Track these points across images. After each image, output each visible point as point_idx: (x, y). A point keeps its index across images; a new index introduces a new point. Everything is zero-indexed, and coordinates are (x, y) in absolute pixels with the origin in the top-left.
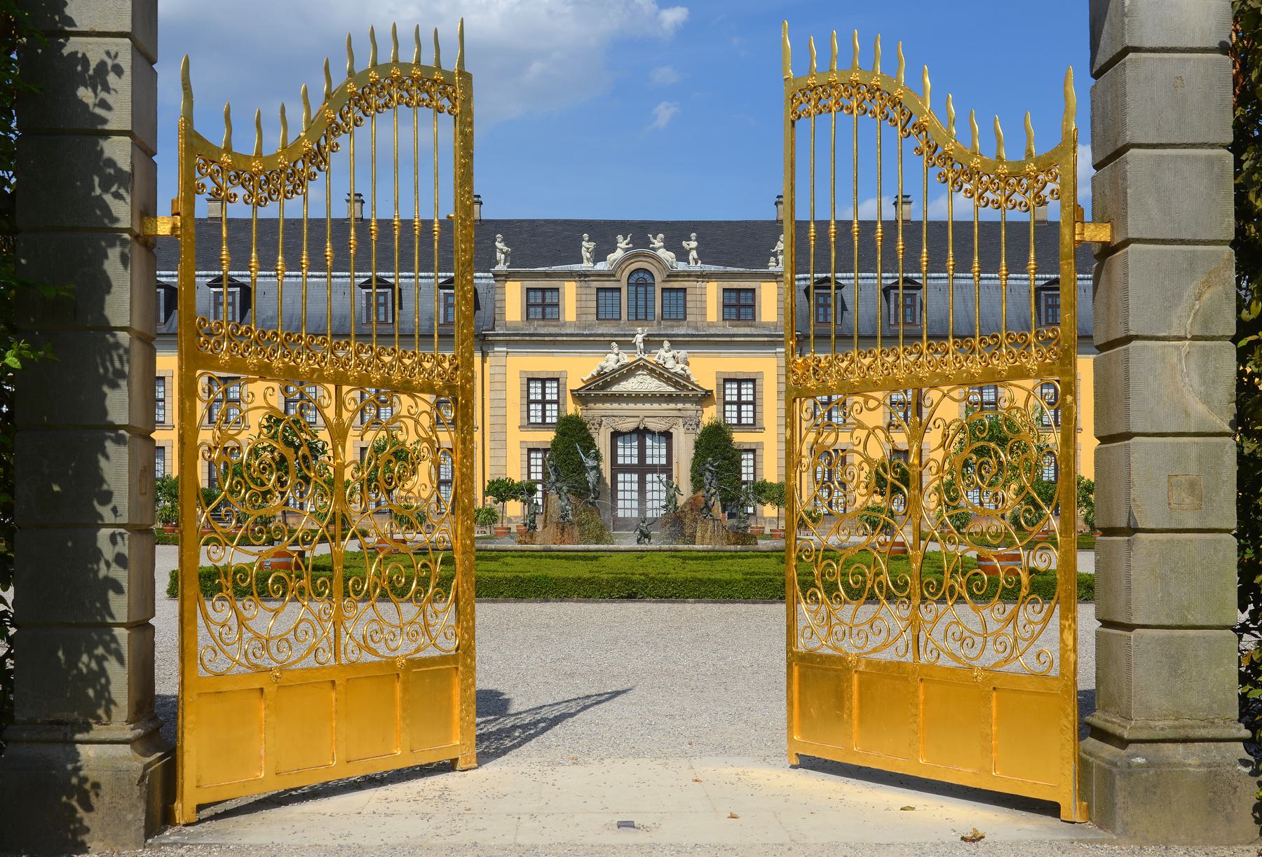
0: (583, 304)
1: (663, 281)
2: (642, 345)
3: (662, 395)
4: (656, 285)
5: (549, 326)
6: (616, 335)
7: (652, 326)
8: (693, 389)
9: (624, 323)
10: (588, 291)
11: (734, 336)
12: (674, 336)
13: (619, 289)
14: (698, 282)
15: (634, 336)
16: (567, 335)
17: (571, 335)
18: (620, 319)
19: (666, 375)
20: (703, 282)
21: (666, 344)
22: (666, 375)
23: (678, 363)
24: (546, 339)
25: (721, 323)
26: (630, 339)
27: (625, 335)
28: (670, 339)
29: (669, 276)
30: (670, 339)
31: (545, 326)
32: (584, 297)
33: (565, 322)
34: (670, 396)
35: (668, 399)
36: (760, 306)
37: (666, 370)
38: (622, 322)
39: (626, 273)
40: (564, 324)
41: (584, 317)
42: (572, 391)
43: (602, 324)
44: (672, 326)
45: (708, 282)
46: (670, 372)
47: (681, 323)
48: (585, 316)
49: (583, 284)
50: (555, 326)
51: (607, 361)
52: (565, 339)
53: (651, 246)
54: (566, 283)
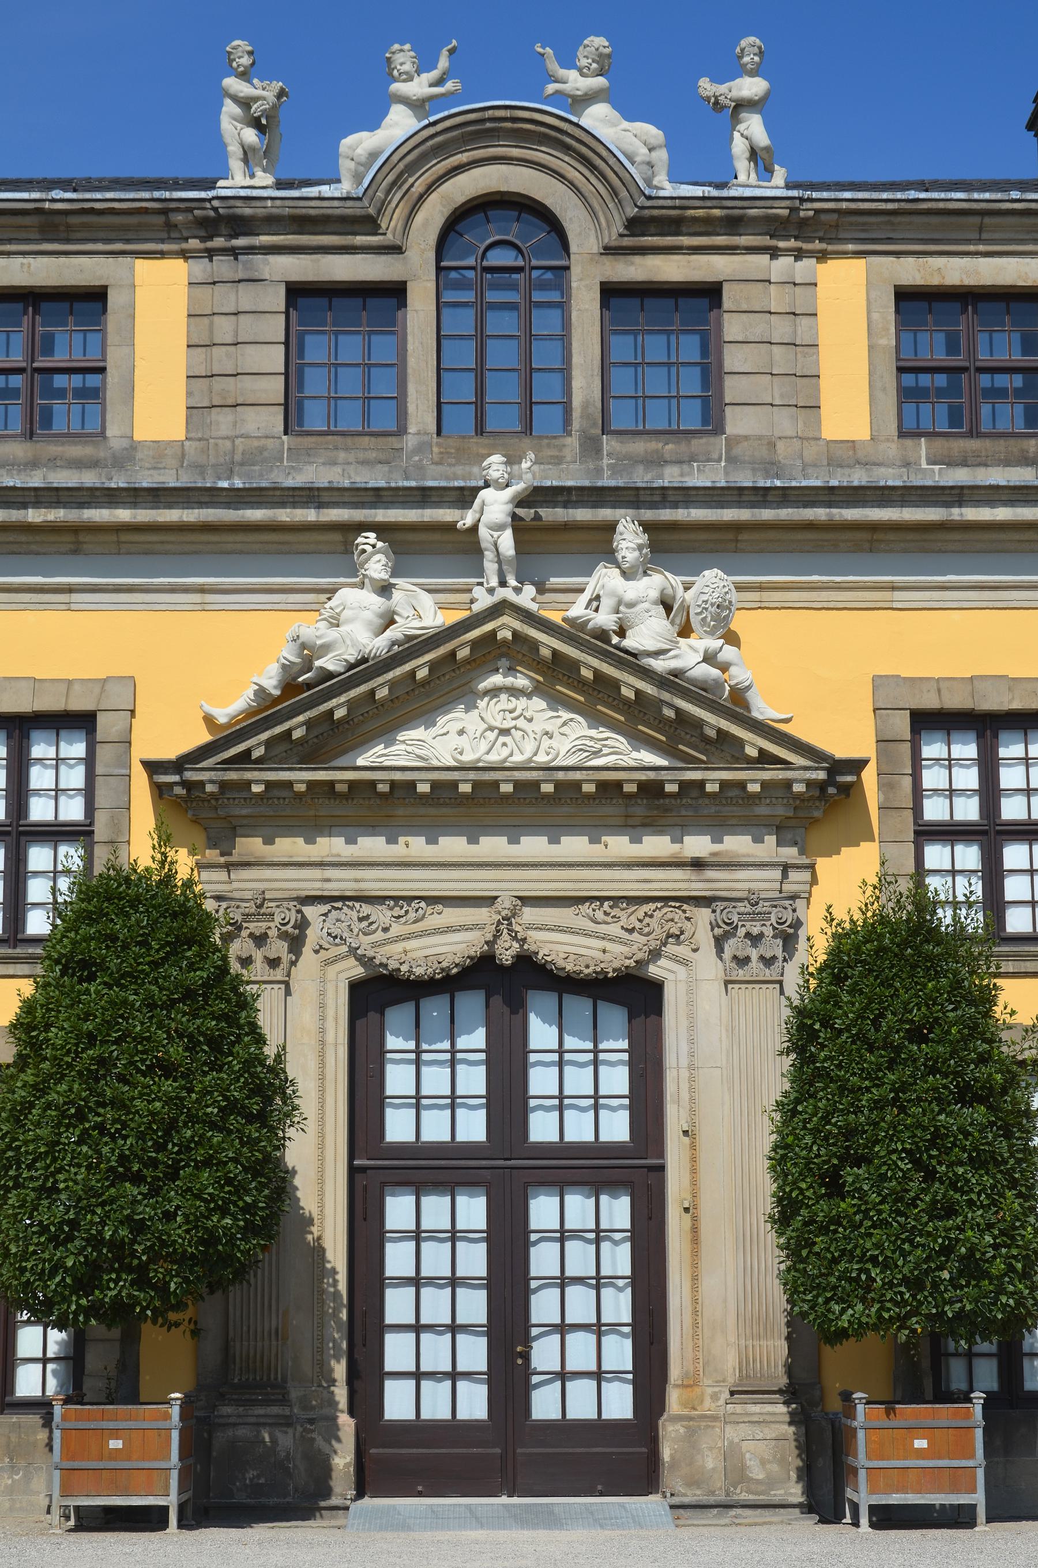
0: (222, 360)
1: (610, 251)
3: (609, 789)
4: (576, 271)
5: (53, 463)
6: (378, 497)
7: (558, 461)
9: (420, 449)
10: (246, 298)
11: (960, 495)
12: (665, 496)
14: (774, 253)
15: (465, 497)
16: (135, 496)
17: (157, 496)
18: (401, 431)
20: (799, 255)
23: (685, 631)
24: (34, 516)
25: (892, 448)
26: (445, 515)
27: (424, 496)
28: (648, 515)
30: (648, 515)
31: (33, 464)
32: (224, 329)
33: (134, 446)
34: (651, 790)
38: (410, 441)
40: (122, 460)
41: (223, 422)
42: (152, 767)
43: (309, 452)
44: (657, 462)
46: (646, 673)
47: (698, 444)
49: (223, 266)
50: (78, 464)
52: (124, 515)
53: (551, 88)
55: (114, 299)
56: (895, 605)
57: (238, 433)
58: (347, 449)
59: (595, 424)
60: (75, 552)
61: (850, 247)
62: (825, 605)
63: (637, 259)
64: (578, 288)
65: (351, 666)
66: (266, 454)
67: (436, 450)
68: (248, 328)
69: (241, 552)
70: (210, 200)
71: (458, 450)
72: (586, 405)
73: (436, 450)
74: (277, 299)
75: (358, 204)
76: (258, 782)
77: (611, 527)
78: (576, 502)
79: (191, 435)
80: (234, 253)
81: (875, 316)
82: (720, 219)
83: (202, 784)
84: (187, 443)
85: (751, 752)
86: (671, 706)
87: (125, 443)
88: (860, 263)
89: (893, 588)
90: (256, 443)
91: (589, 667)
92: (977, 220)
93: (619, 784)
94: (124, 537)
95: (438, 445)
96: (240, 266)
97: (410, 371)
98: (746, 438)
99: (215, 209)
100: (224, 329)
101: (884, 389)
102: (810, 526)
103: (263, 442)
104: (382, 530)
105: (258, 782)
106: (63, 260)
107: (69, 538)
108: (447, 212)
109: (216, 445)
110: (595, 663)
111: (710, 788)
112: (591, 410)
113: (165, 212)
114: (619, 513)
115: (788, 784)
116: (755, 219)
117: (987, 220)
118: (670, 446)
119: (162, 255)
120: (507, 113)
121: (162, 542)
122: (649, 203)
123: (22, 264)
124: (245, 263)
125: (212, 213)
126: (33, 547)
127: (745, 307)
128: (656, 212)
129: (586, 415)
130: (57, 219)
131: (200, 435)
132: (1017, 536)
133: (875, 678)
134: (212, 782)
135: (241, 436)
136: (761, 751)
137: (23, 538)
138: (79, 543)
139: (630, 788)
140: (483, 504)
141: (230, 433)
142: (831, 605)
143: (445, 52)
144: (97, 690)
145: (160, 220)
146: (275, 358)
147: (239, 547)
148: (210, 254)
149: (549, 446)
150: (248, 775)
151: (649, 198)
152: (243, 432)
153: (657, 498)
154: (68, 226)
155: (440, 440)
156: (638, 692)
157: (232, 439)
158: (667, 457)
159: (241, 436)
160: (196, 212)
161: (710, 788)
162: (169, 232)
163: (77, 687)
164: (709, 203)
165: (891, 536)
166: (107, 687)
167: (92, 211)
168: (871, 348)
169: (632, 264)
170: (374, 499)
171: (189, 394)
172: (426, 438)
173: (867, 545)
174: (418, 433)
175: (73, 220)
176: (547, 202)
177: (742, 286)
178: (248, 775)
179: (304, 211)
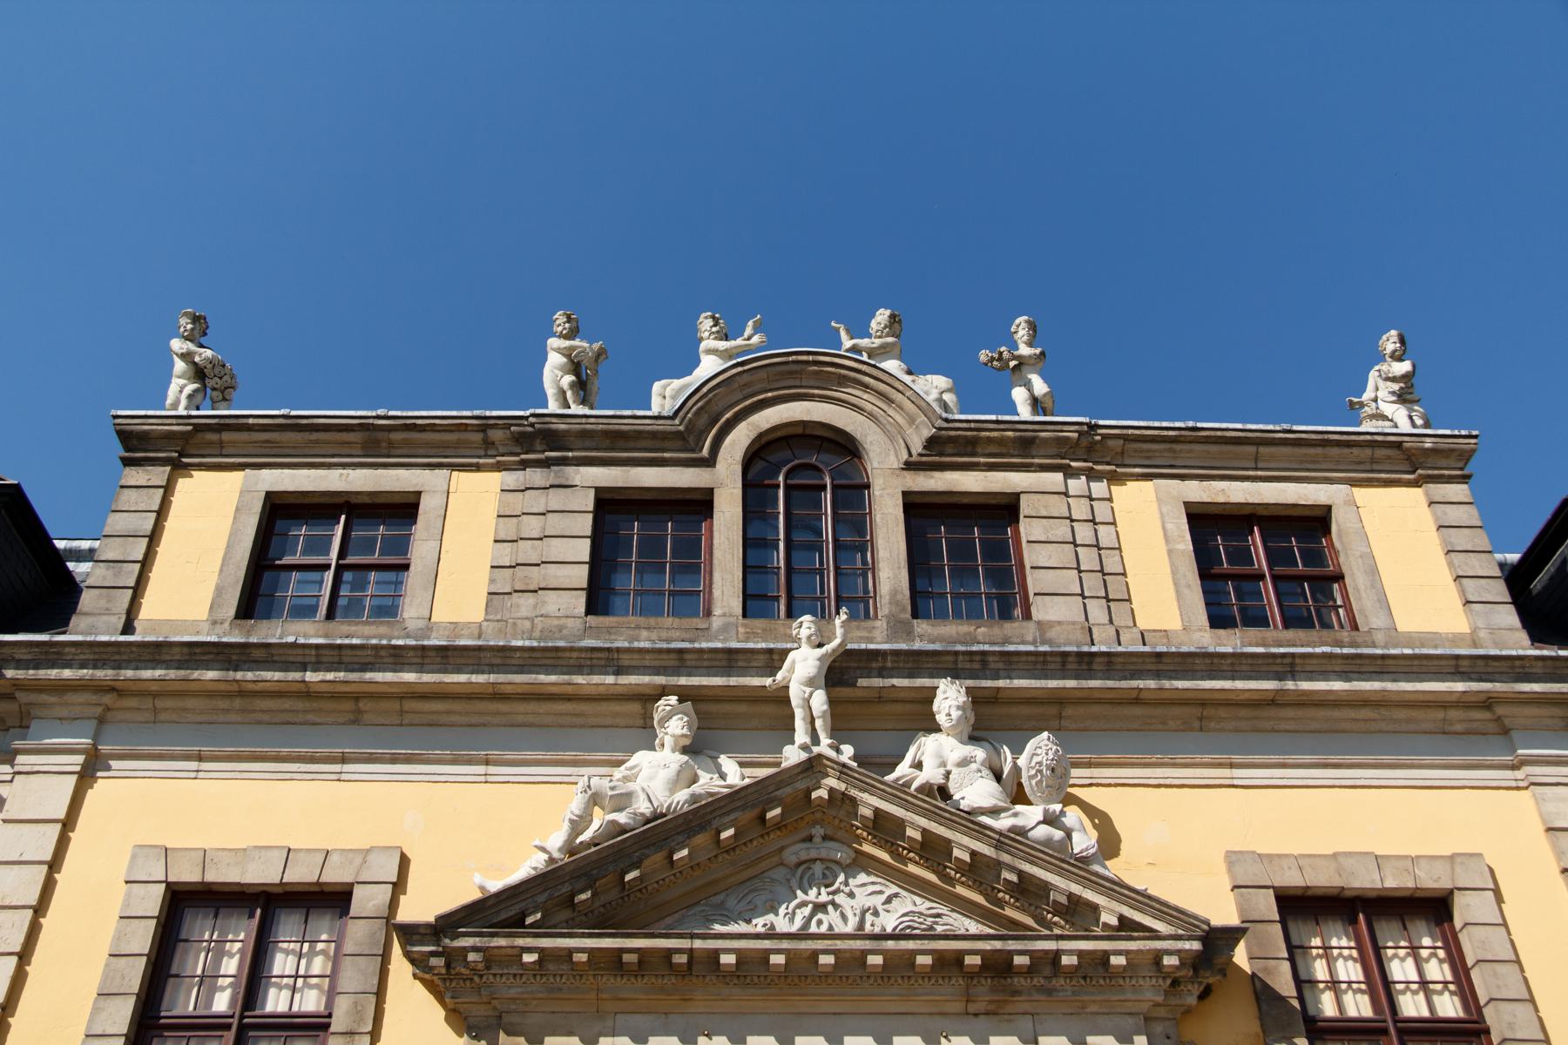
0: (527, 551)
1: (910, 466)
2: (819, 700)
6: (681, 660)
8: (1126, 927)
10: (556, 499)
13: (700, 504)
14: (1069, 473)
15: (773, 660)
19: (964, 845)
20: (1092, 476)
21: (949, 698)
22: (964, 845)
27: (730, 660)
29: (931, 443)
32: (532, 526)
34: (998, 966)
35: (984, 992)
36: (1373, 571)
37: (969, 820)
39: (740, 439)
41: (525, 604)
42: (409, 933)
45: (1115, 479)
46: (981, 831)
48: (529, 600)
49: (536, 476)
51: (604, 1028)
54: (462, 480)
55: (426, 504)
56: (1236, 782)
57: (538, 613)
58: (648, 628)
59: (904, 610)
60: (355, 722)
61: (1137, 470)
62: (1162, 782)
63: (937, 474)
64: (881, 496)
65: (648, 821)
66: (565, 632)
67: (741, 630)
68: (555, 524)
69: (532, 725)
70: (526, 418)
71: (764, 630)
72: (894, 593)
73: (741, 630)
74: (589, 502)
75: (669, 422)
76: (530, 950)
77: (929, 696)
78: (893, 668)
79: (488, 618)
80: (546, 464)
81: (1169, 526)
82: (1015, 440)
83: (465, 950)
84: (485, 624)
85: (1109, 918)
86: (1012, 869)
87: (421, 624)
88: (1148, 486)
89: (1232, 766)
90: (556, 622)
91: (915, 826)
92: (1251, 449)
93: (959, 956)
94: (409, 705)
95: (744, 626)
96: (552, 474)
97: (715, 561)
98: (1059, 623)
99: (532, 425)
100: (532, 526)
101: (1189, 586)
102: (1137, 699)
103: (563, 621)
104: (685, 695)
105: (530, 950)
106: (380, 472)
107: (349, 705)
108: (753, 435)
109: (515, 624)
110: (923, 822)
111: (1065, 960)
112: (899, 597)
113: (483, 429)
114: (934, 682)
115: (1157, 956)
116: (1046, 440)
117: (1262, 449)
118: (982, 630)
119: (478, 468)
120: (811, 358)
121: (448, 713)
122: (946, 425)
123: (341, 475)
124: (556, 473)
125: (530, 429)
126: (310, 717)
127: (1044, 513)
128: (953, 433)
129: (894, 601)
130: (380, 435)
131: (499, 617)
132: (1352, 714)
133: (1229, 854)
134: (475, 949)
135: (541, 616)
136: (1121, 918)
137: (300, 705)
138: (359, 711)
139: (973, 961)
140: (794, 662)
141: (529, 615)
142: (1168, 782)
143: (750, 323)
144: (358, 860)
145: (478, 437)
146: (583, 550)
147: (531, 719)
148: (524, 465)
149: (858, 628)
150: (520, 942)
151: (947, 420)
152: (543, 612)
153: (976, 666)
154: (391, 444)
155: (746, 621)
156: (973, 854)
157: (532, 620)
158: (980, 638)
159: (541, 616)
160: (513, 428)
161: (1065, 960)
162: (486, 450)
163: (334, 858)
164: (1002, 426)
165: (1222, 712)
166: (372, 857)
167: (414, 428)
168: (1170, 552)
169: (932, 477)
170: (676, 663)
171: (492, 581)
172: (732, 620)
173: (1197, 724)
174: (724, 615)
175: (396, 436)
176: (848, 429)
177: (1039, 496)
178: (520, 942)
179: (617, 427)
